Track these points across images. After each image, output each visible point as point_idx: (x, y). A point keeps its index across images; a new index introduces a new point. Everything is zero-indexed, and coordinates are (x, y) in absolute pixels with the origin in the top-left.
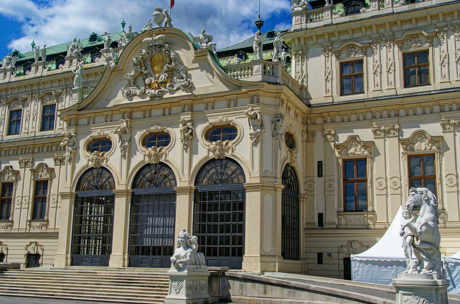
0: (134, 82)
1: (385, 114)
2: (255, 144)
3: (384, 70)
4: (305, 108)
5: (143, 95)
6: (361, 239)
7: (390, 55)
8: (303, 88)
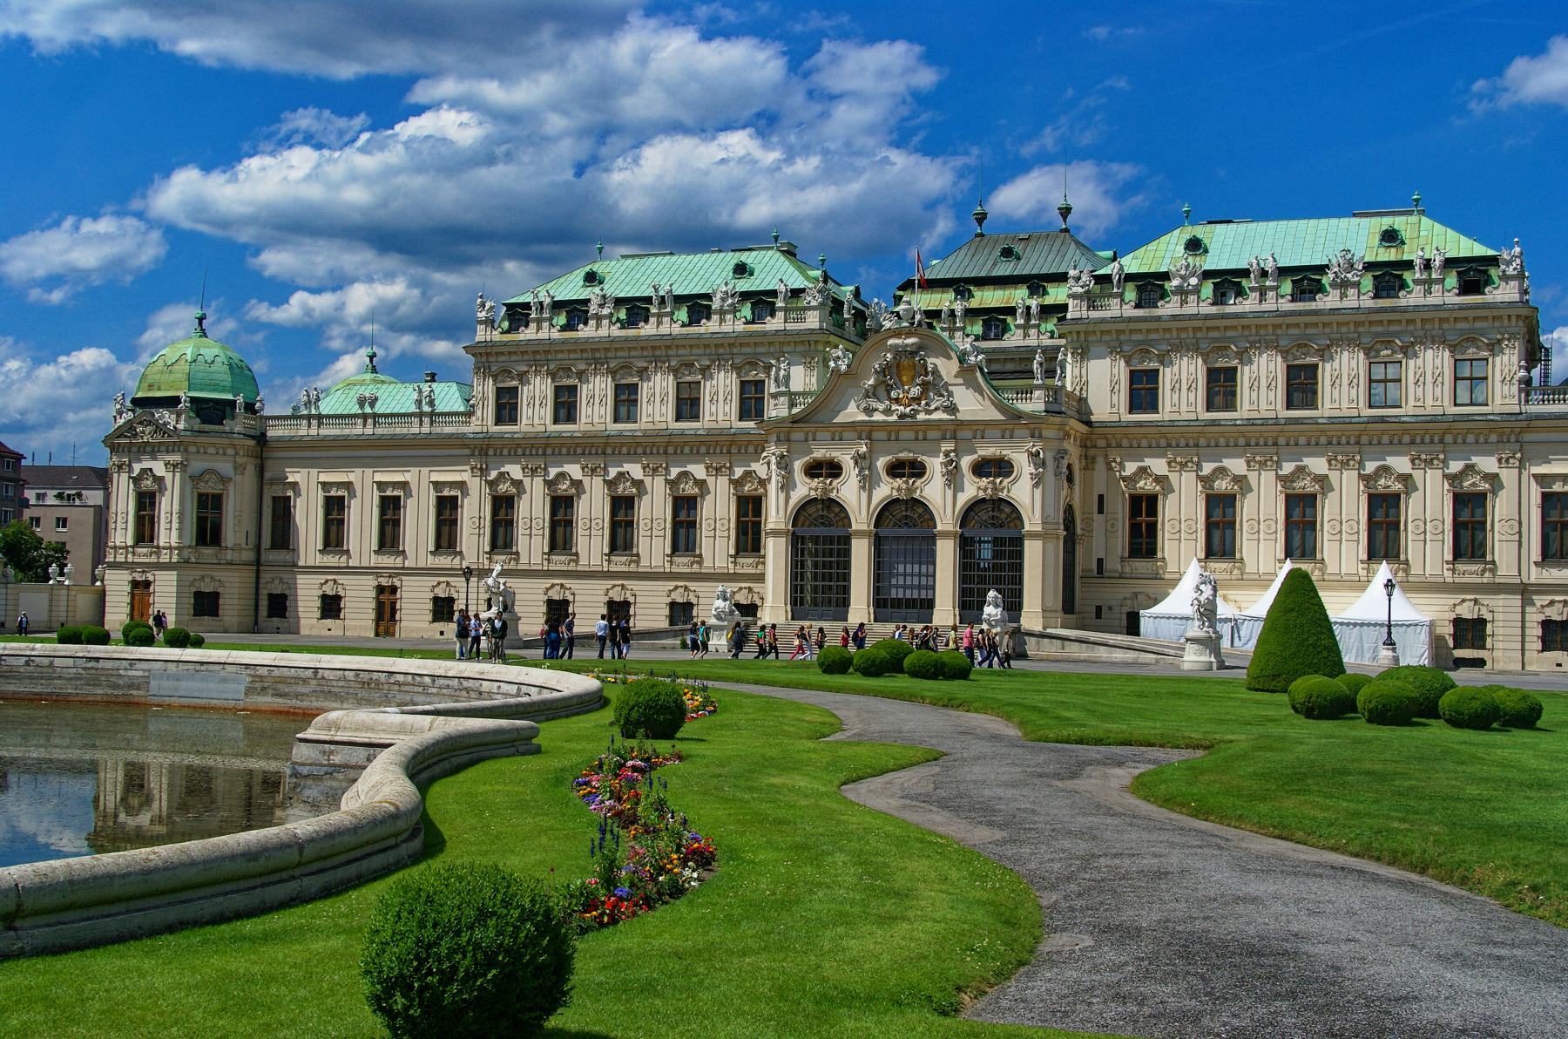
0: (872, 393)
1: (1183, 442)
2: (1036, 485)
3: (1184, 387)
4: (1084, 429)
5: (888, 412)
6: (1149, 591)
7: (1192, 368)
8: (1082, 401)
